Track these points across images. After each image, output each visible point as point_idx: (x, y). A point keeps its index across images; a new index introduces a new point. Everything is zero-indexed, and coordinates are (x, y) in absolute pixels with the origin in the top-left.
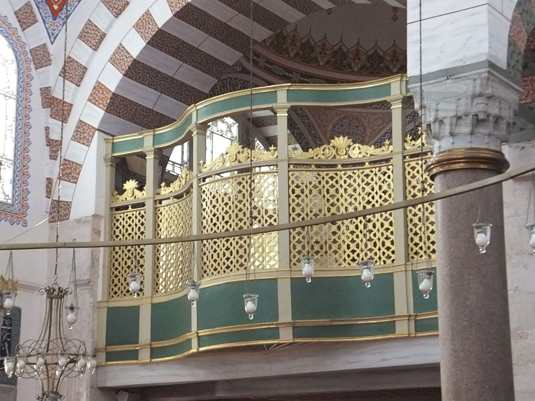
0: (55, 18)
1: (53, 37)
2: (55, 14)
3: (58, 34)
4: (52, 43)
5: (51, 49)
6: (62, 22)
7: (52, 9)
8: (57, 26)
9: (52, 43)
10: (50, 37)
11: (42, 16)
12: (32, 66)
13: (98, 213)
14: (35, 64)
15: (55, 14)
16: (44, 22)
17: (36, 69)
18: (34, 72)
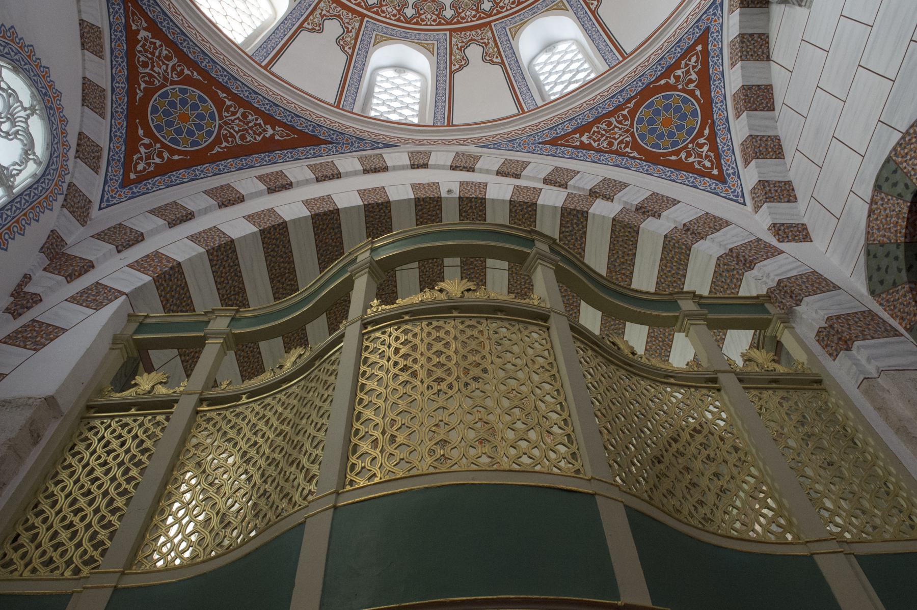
0: (123, 186)
1: (106, 203)
2: (126, 183)
3: (115, 204)
4: (100, 209)
5: (95, 212)
6: (130, 195)
7: (126, 175)
8: (120, 195)
9: (100, 209)
10: (102, 201)
11: (106, 175)
12: (61, 198)
13: (60, 401)
14: (65, 200)
15: (126, 183)
16: (106, 182)
17: (63, 206)
18: (57, 205)
